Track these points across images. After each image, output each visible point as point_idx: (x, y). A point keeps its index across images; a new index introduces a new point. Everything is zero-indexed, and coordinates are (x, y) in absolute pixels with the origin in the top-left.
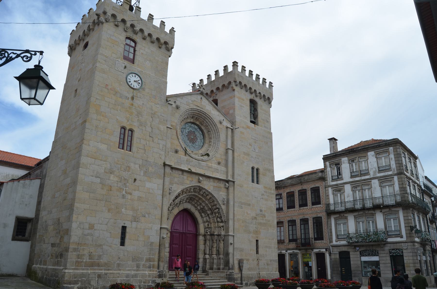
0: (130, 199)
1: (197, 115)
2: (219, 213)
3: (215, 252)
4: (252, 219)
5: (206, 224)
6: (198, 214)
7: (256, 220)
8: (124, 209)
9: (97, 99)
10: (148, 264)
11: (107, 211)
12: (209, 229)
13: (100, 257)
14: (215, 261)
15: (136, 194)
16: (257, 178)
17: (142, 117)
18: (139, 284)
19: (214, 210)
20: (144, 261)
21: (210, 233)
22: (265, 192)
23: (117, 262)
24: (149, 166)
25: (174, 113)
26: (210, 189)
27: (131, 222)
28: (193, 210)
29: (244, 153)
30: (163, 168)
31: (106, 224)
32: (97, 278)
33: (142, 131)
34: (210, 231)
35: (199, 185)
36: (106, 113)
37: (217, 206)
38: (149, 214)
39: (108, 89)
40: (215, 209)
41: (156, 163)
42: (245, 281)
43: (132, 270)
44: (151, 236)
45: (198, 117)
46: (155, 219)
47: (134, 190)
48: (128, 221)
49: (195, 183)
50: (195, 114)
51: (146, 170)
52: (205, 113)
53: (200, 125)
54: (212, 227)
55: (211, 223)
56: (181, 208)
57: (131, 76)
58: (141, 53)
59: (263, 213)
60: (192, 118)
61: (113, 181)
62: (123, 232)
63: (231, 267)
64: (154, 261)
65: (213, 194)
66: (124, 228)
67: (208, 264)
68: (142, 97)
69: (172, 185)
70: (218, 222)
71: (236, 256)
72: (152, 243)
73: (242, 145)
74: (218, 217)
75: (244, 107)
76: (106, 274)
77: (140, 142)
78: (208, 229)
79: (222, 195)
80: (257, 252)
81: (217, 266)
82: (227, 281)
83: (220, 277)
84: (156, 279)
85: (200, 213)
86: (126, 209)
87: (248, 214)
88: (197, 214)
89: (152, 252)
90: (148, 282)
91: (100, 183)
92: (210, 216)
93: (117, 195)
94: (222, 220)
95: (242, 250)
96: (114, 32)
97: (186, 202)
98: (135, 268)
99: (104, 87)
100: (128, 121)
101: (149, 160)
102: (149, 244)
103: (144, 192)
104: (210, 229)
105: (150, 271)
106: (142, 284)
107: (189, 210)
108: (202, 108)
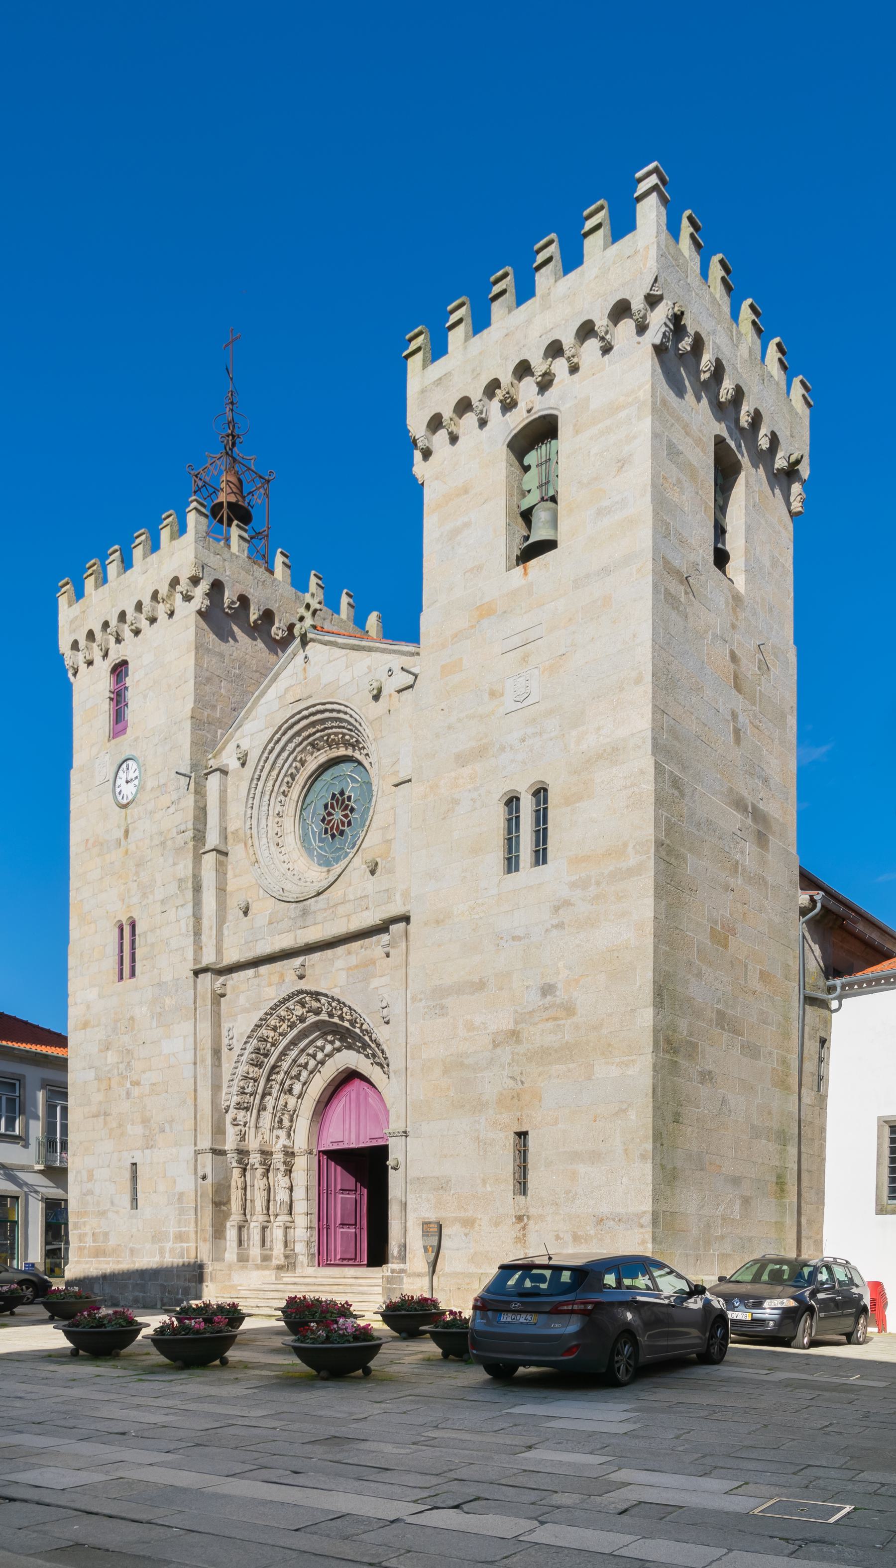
7: (518, 1041)
26: (336, 986)
30: (191, 980)
46: (184, 1131)
49: (292, 985)
56: (330, 1071)
59: (561, 995)
72: (181, 1195)
79: (377, 988)
80: (522, 1186)
95: (442, 1185)
102: (177, 1197)
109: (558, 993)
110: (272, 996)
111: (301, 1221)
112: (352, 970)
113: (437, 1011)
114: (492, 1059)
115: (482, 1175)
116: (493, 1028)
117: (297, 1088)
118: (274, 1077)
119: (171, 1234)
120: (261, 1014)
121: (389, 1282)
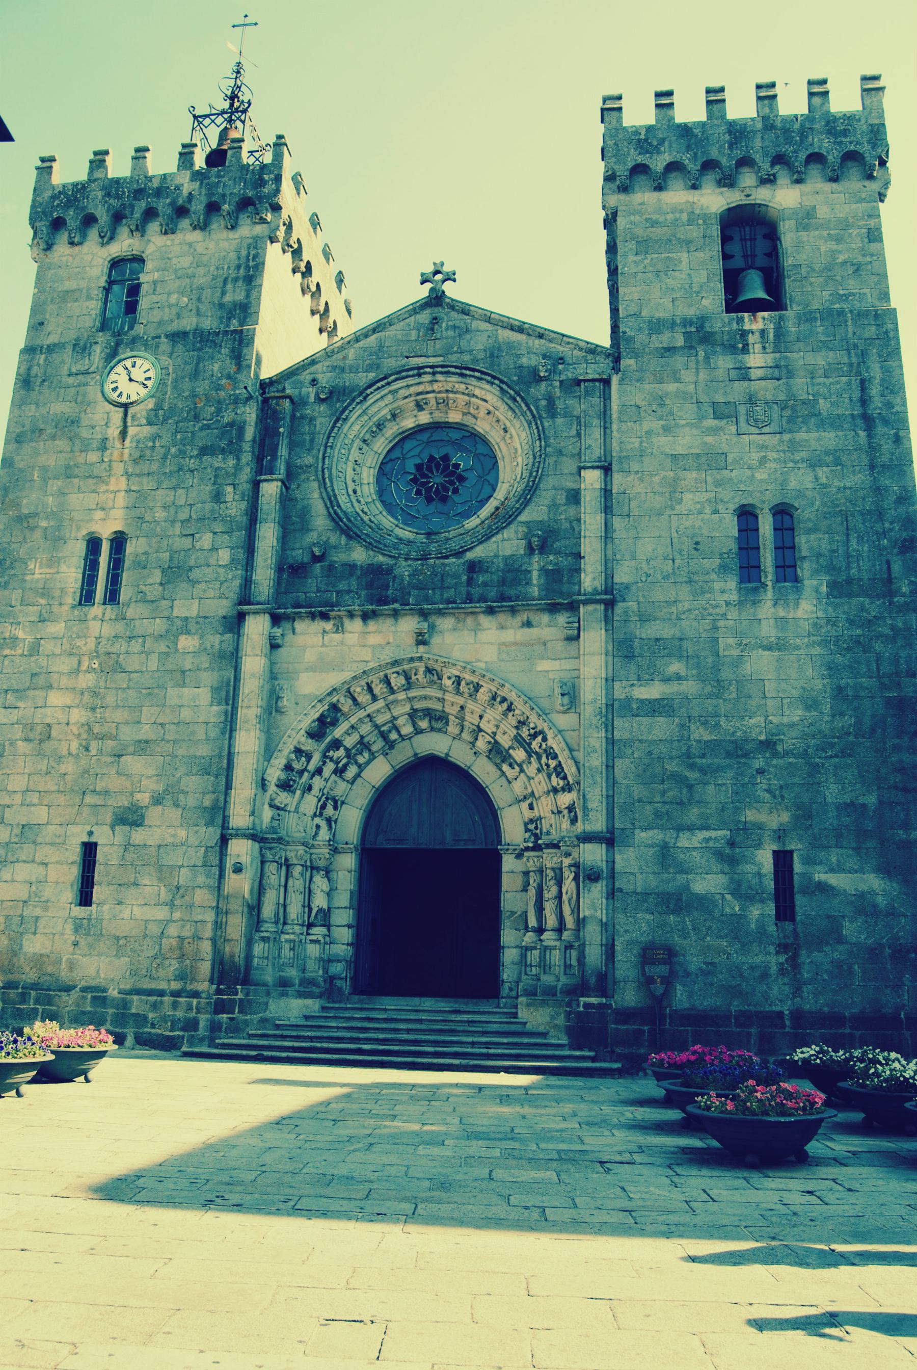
1: (433, 391)
5: (525, 805)
6: (490, 767)
26: (478, 661)
28: (461, 755)
45: (439, 395)
50: (420, 388)
51: (167, 650)
52: (456, 367)
53: (468, 421)
56: (403, 755)
60: (419, 407)
62: (90, 861)
66: (89, 849)
70: (555, 791)
79: (547, 671)
94: (565, 778)
97: (418, 731)
111: (344, 935)
112: (506, 646)
117: (352, 771)
118: (331, 753)
120: (347, 675)
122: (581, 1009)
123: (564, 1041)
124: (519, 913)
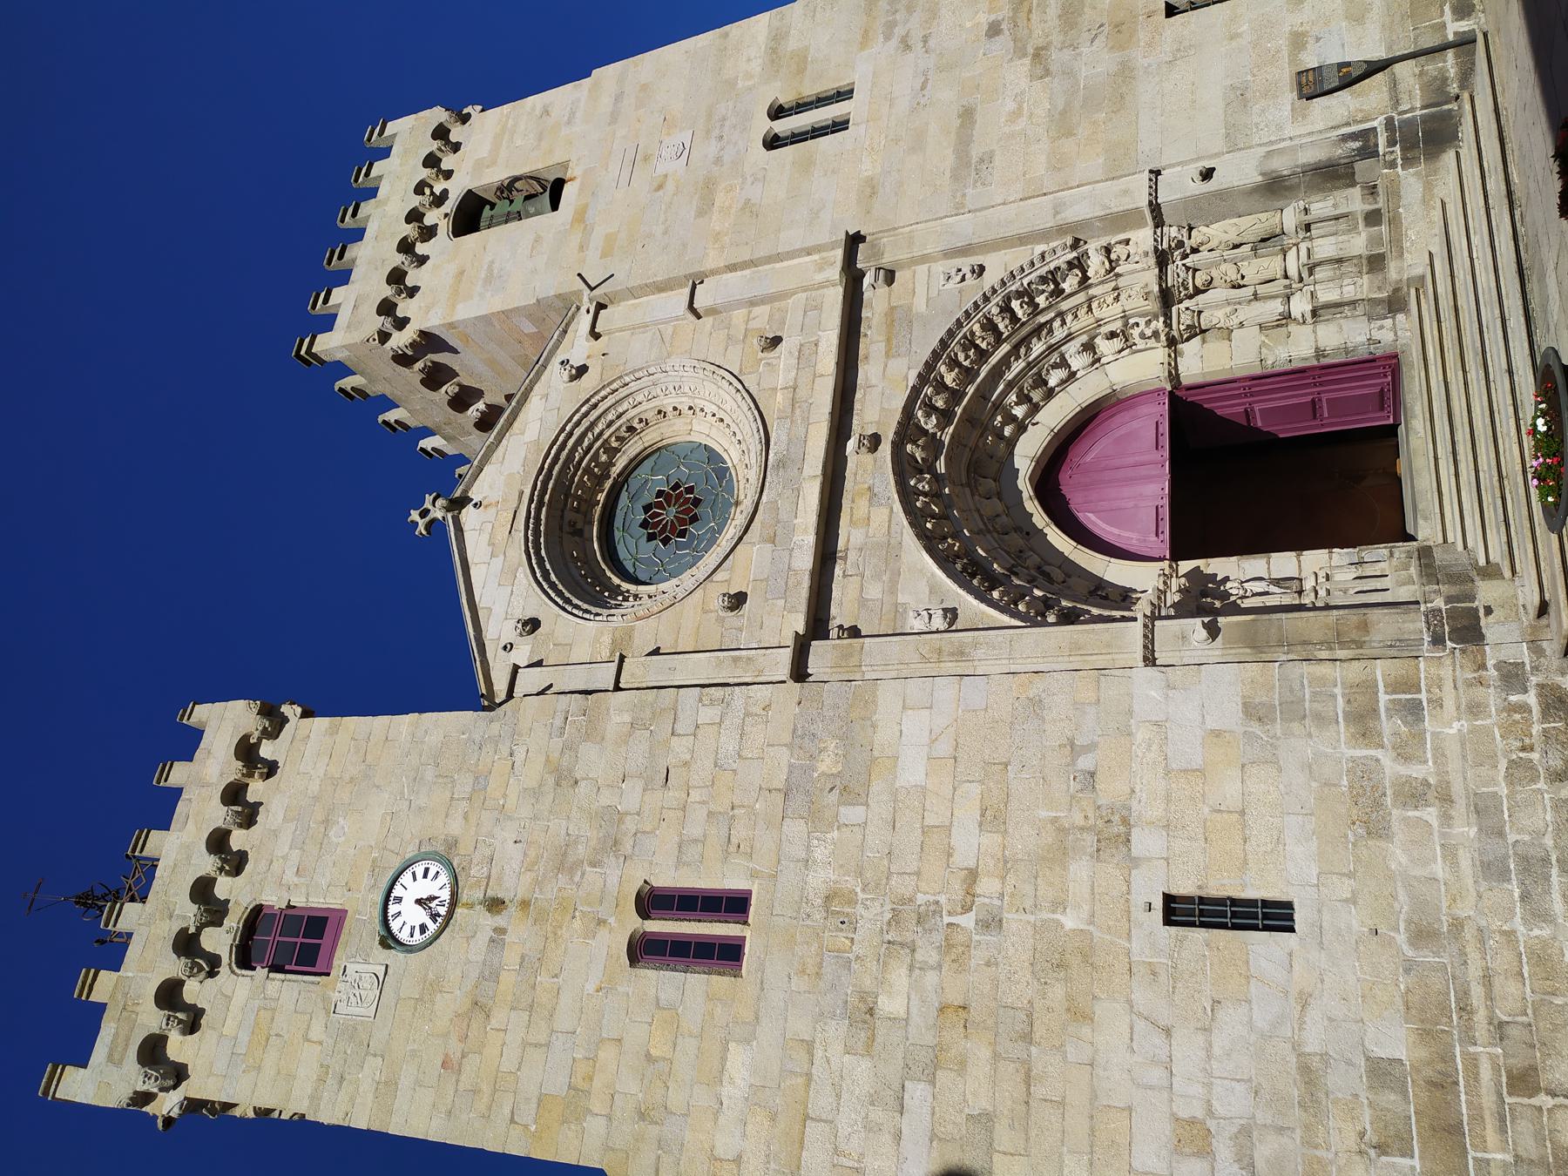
0: (1003, 878)
1: (563, 511)
2: (1027, 295)
3: (1264, 262)
4: (1047, 73)
8: (1062, 918)
9: (512, 1121)
10: (1389, 726)
11: (1086, 1031)
12: (1137, 324)
13: (1382, 1072)
14: (1325, 247)
15: (969, 843)
16: (821, 101)
17: (576, 842)
18: (1541, 785)
19: (1023, 324)
20: (1379, 753)
21: (1156, 317)
22: (887, 38)
23: (1405, 947)
24: (816, 775)
25: (554, 645)
26: (906, 378)
27: (1135, 862)
29: (701, 213)
31: (1168, 1032)
32: (1535, 1101)
33: (644, 832)
34: (1142, 321)
35: (886, 449)
36: (574, 1059)
37: (995, 310)
38: (1072, 745)
39: (463, 1057)
40: (1014, 318)
41: (794, 731)
42: (1444, 25)
43: (1443, 835)
44: (1203, 723)
47: (950, 855)
48: (1128, 883)
52: (539, 473)
54: (1116, 309)
55: (1099, 323)
57: (399, 921)
58: (296, 880)
61: (913, 997)
63: (1357, 144)
64: (1369, 687)
65: (925, 355)
66: (1176, 911)
67: (1349, 292)
68: (488, 852)
69: (905, 611)
71: (1280, 128)
72: (1253, 711)
73: (665, 233)
74: (1058, 292)
75: (492, 262)
76: (1500, 1030)
77: (696, 841)
78: (1136, 332)
81: (1354, 229)
82: (1451, 154)
83: (1425, 202)
84: (1490, 663)
85: (1050, 394)
86: (1059, 905)
87: (1016, 114)
88: (1055, 415)
89: (1307, 705)
90: (1517, 716)
91: (933, 1083)
92: (1059, 333)
93: (988, 964)
94: (1069, 263)
95: (1240, 97)
96: (221, 1035)
98: (1431, 814)
99: (457, 1081)
100: (601, 922)
101: (779, 781)
102: (1256, 728)
103: (955, 789)
104: (1132, 321)
105: (1438, 703)
106: (1535, 756)
107: (1037, 462)
108: (521, 493)
109: (1000, 18)
110: (886, 511)
113: (985, 167)
114: (1064, 73)
115: (1225, 43)
116: (1024, 83)
119: (1359, 753)
121: (1414, 146)
122: (1397, 148)
123: (1449, 157)
124: (1263, 338)
